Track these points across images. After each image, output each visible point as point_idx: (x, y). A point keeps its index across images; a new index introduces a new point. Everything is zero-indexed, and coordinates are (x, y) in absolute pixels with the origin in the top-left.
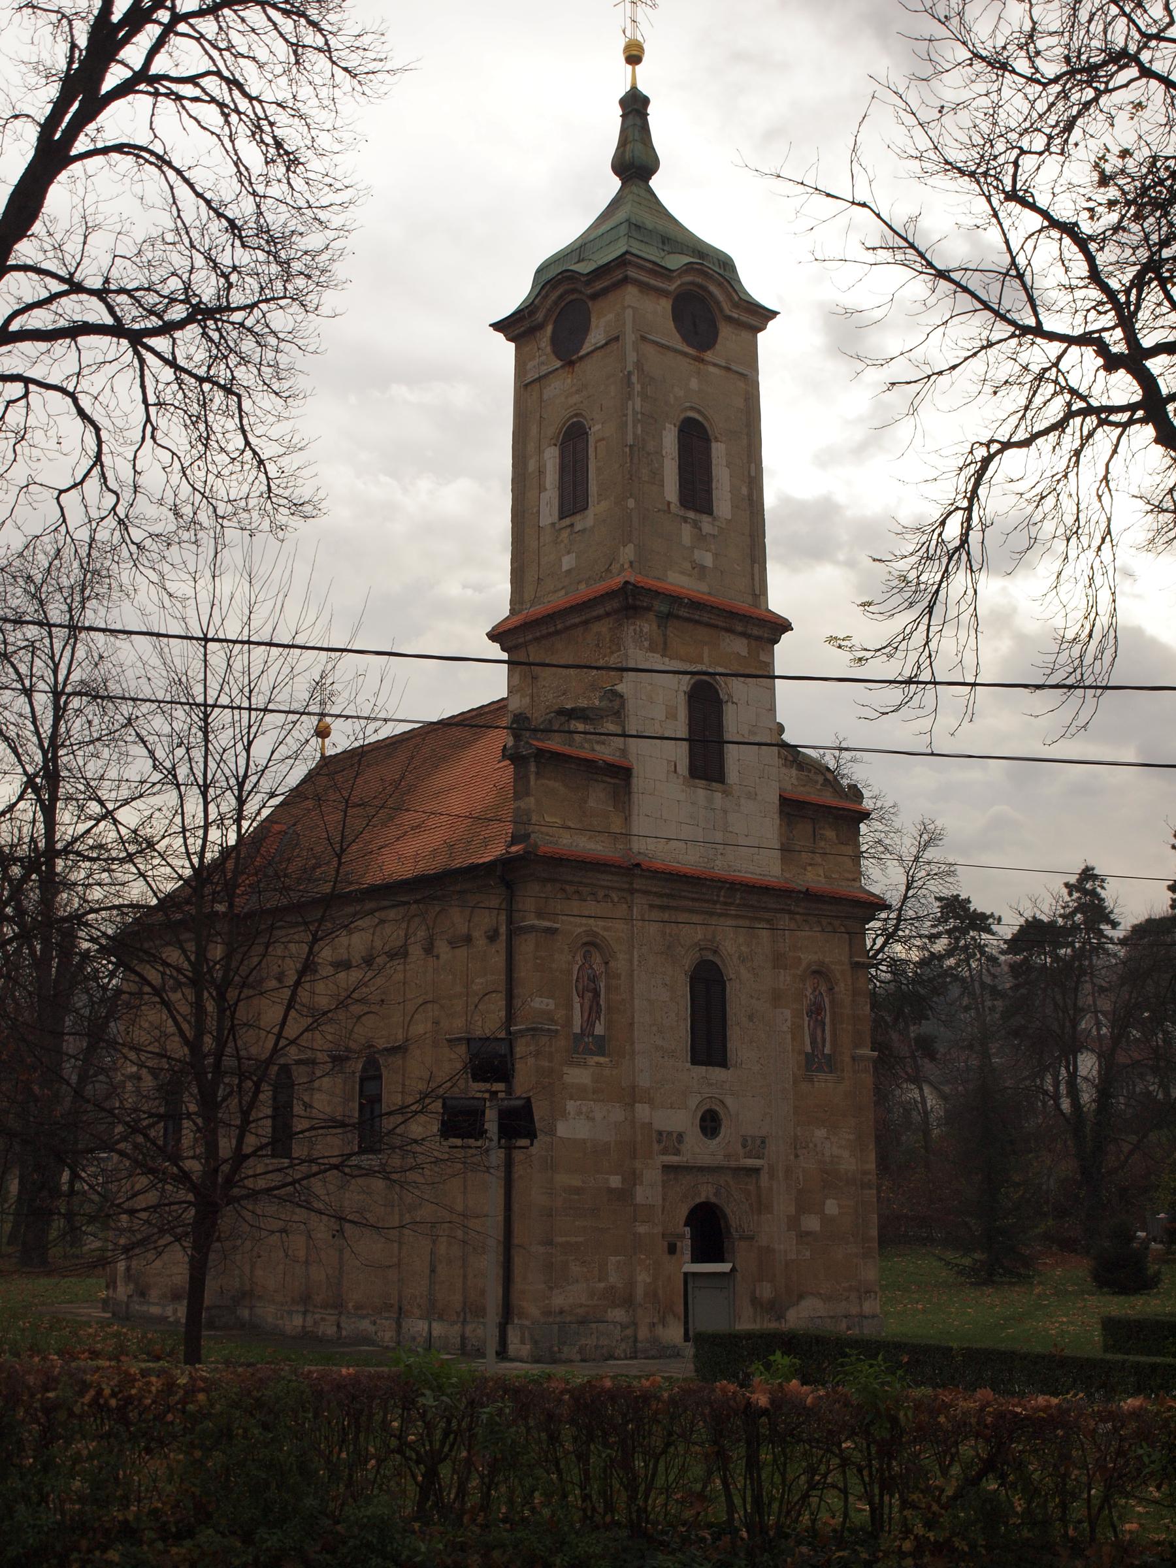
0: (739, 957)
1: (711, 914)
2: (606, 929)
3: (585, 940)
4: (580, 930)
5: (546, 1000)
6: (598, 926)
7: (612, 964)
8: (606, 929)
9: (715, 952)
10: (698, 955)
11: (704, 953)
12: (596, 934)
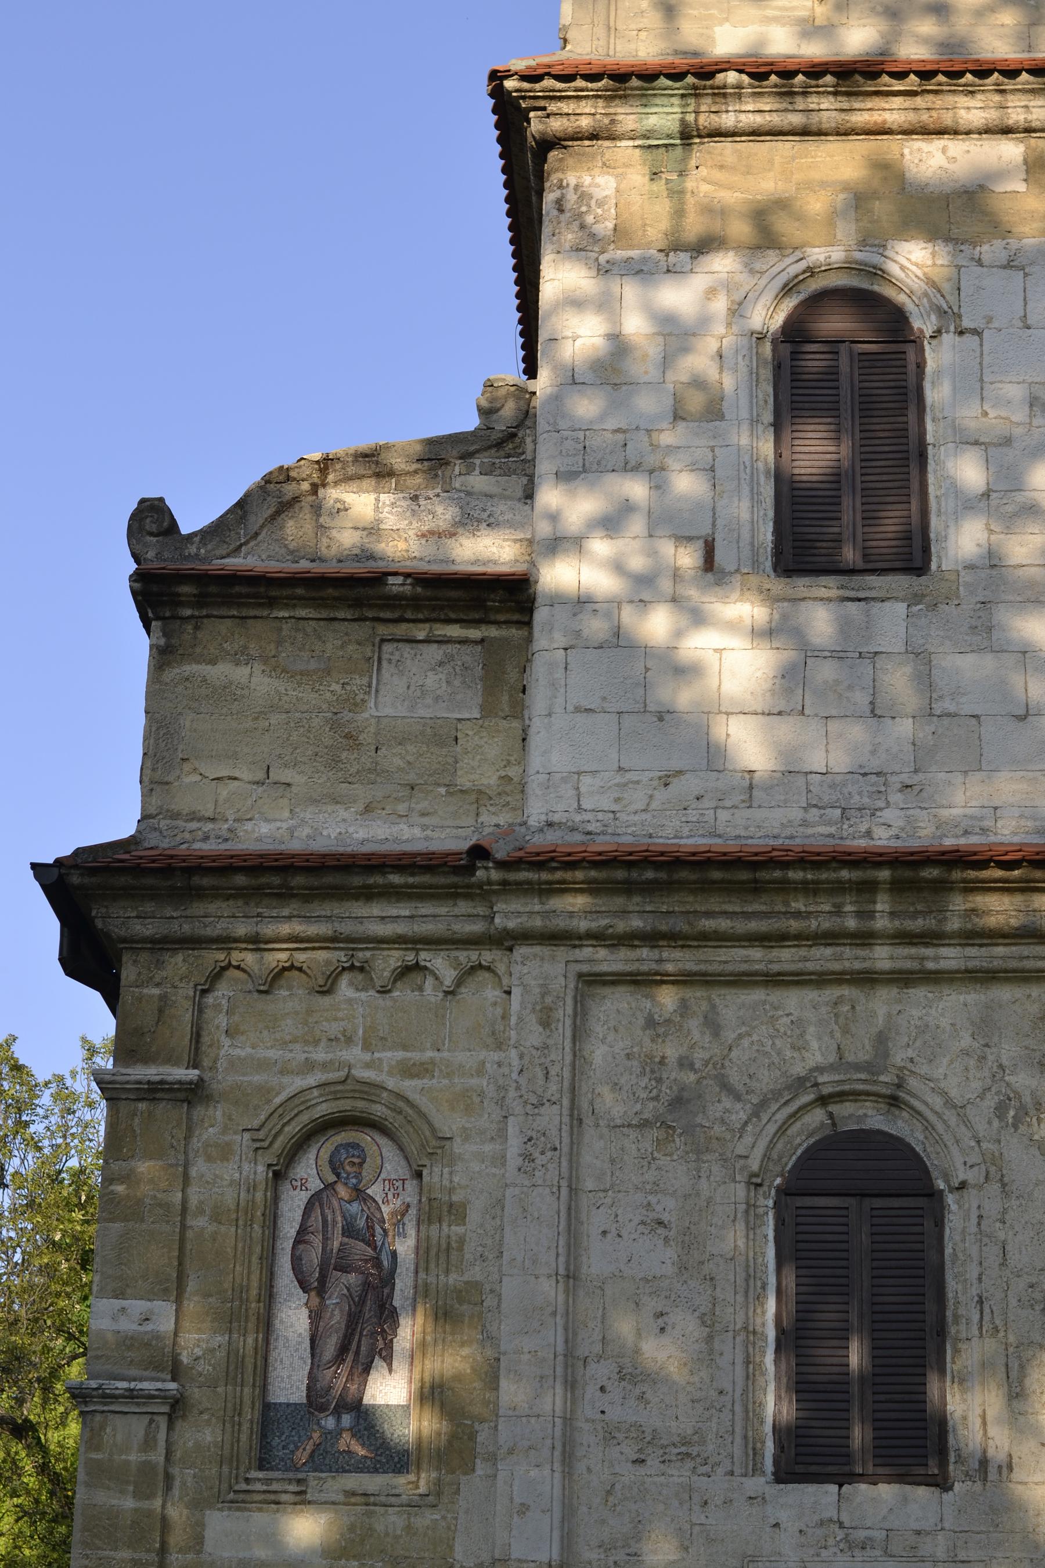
0: (1000, 1110)
1: (867, 979)
2: (409, 1070)
3: (324, 1109)
4: (311, 1080)
5: (137, 1306)
6: (377, 1067)
7: (434, 1175)
8: (409, 1070)
9: (894, 1102)
10: (817, 1117)
11: (843, 1109)
12: (370, 1090)
